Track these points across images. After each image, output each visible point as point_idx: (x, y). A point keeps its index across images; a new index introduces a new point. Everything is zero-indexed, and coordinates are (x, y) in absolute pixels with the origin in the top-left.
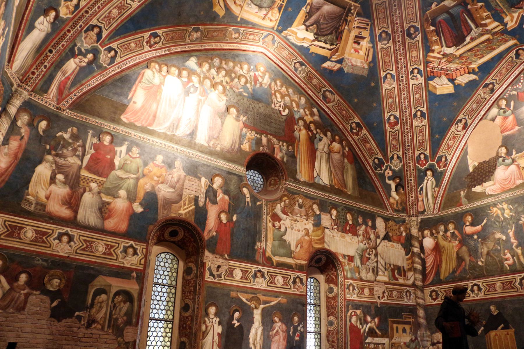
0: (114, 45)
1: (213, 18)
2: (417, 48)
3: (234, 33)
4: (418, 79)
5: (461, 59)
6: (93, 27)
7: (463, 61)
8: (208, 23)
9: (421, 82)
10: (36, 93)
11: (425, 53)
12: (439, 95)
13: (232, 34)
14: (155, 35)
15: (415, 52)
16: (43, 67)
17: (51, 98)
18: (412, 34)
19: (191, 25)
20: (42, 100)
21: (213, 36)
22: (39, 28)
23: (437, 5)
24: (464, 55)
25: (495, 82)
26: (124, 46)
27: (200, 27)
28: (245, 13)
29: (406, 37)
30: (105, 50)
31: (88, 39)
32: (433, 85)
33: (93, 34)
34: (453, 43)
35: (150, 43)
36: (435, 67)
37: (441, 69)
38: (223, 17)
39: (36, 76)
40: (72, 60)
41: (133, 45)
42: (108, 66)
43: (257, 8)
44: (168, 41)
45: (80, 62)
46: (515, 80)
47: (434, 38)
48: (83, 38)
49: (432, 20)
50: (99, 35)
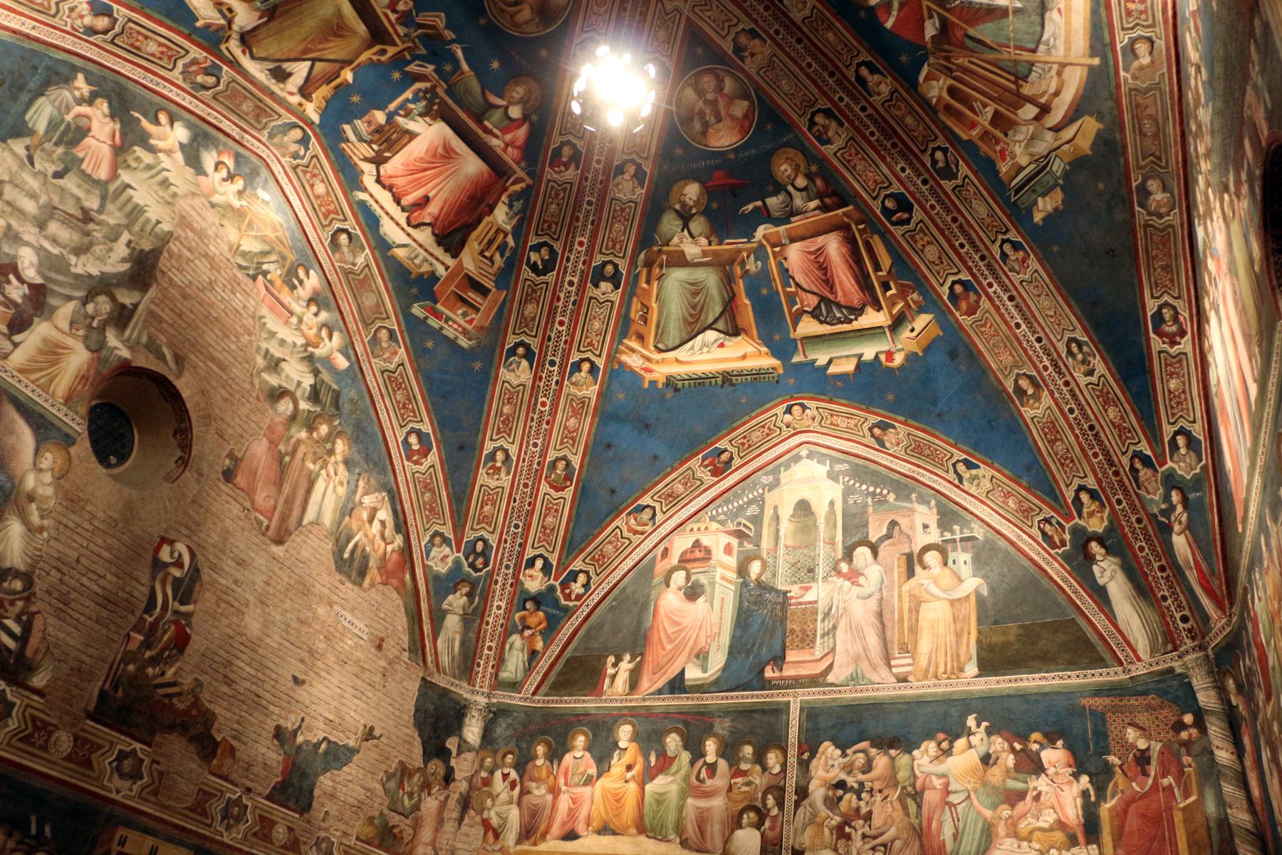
0: (1168, 431)
1: (1108, 146)
3: (1136, 64)
6: (1134, 470)
8: (1122, 160)
13: (1141, 68)
14: (1158, 319)
19: (1133, 216)
21: (1156, 135)
26: (1172, 408)
27: (1134, 184)
28: (1074, 48)
33: (1144, 473)
35: (1174, 335)
38: (1100, 118)
41: (1173, 384)
42: (1201, 460)
43: (1047, 15)
44: (1172, 280)
45: (1180, 523)
48: (1149, 497)
50: (1146, 461)
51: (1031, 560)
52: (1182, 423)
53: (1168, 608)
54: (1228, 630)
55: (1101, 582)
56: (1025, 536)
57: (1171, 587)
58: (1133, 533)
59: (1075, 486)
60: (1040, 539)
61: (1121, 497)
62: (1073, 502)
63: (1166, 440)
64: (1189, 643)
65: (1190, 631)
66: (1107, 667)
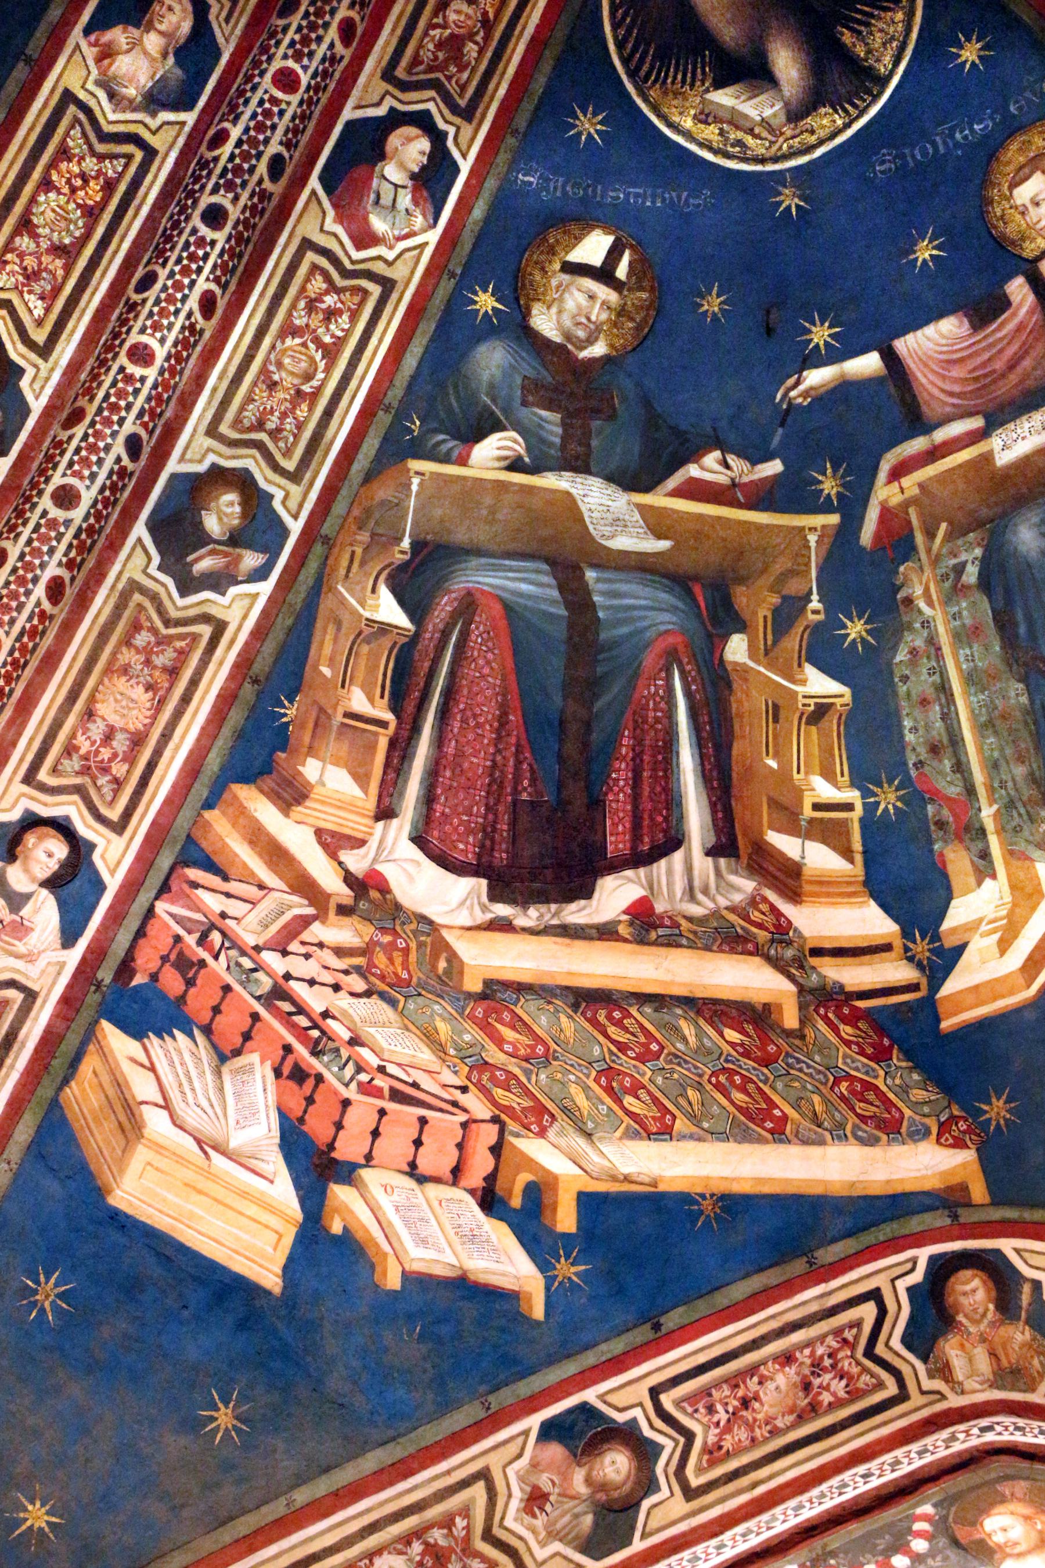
2: (173, 672)
4: (21, 929)
5: (485, 1027)
7: (494, 1055)
9: (32, 975)
11: (214, 762)
12: (120, 1221)
15: (139, 694)
18: (202, 539)
23: (515, 465)
24: (527, 1008)
25: (668, 1445)
29: (140, 530)
32: (120, 1085)
34: (486, 849)
36: (231, 941)
37: (279, 993)
46: (855, 1529)
47: (358, 701)
49: (417, 546)
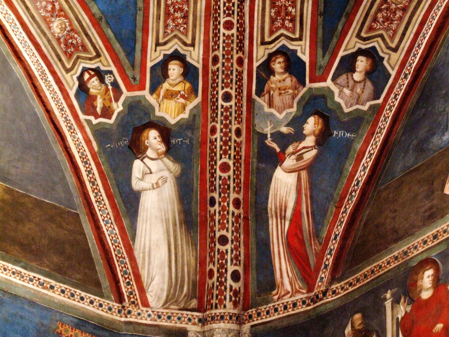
10: (256, 305)
16: (218, 246)
17: (289, 288)
20: (276, 310)
22: (148, 186)
26: (375, 20)
30: (333, 79)
31: (277, 100)
39: (216, 275)
40: (279, 173)
42: (377, 97)
45: (300, 158)
48: (267, 109)
51: (48, 111)
52: (377, 44)
53: (222, 255)
54: (301, 309)
55: (136, 185)
56: (50, 78)
57: (237, 230)
58: (225, 143)
59: (169, 49)
60: (72, 93)
61: (233, 93)
62: (153, 68)
63: (341, 53)
64: (230, 308)
65: (236, 293)
66: (102, 296)
